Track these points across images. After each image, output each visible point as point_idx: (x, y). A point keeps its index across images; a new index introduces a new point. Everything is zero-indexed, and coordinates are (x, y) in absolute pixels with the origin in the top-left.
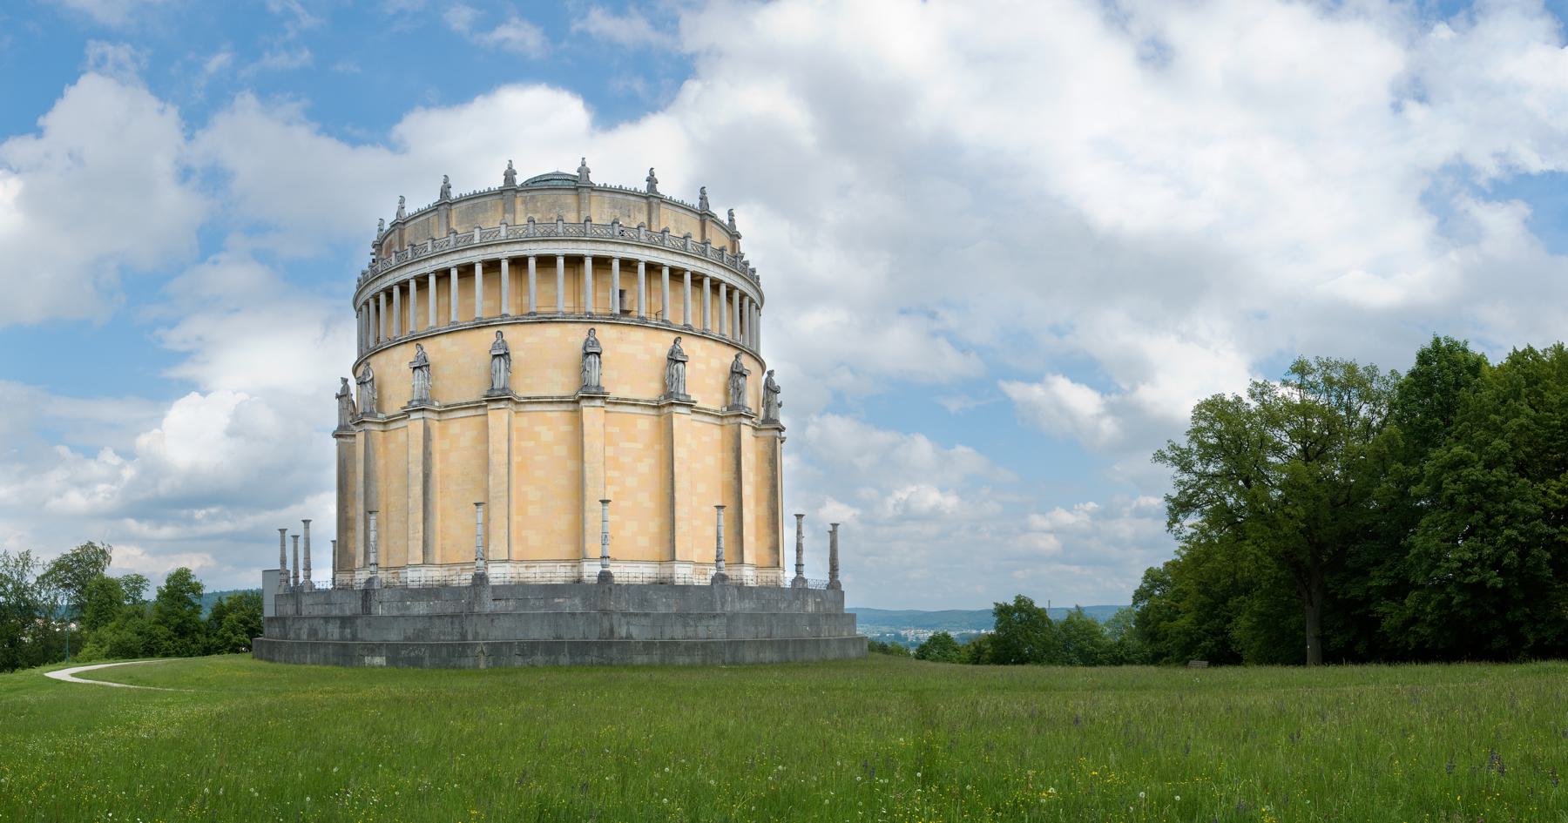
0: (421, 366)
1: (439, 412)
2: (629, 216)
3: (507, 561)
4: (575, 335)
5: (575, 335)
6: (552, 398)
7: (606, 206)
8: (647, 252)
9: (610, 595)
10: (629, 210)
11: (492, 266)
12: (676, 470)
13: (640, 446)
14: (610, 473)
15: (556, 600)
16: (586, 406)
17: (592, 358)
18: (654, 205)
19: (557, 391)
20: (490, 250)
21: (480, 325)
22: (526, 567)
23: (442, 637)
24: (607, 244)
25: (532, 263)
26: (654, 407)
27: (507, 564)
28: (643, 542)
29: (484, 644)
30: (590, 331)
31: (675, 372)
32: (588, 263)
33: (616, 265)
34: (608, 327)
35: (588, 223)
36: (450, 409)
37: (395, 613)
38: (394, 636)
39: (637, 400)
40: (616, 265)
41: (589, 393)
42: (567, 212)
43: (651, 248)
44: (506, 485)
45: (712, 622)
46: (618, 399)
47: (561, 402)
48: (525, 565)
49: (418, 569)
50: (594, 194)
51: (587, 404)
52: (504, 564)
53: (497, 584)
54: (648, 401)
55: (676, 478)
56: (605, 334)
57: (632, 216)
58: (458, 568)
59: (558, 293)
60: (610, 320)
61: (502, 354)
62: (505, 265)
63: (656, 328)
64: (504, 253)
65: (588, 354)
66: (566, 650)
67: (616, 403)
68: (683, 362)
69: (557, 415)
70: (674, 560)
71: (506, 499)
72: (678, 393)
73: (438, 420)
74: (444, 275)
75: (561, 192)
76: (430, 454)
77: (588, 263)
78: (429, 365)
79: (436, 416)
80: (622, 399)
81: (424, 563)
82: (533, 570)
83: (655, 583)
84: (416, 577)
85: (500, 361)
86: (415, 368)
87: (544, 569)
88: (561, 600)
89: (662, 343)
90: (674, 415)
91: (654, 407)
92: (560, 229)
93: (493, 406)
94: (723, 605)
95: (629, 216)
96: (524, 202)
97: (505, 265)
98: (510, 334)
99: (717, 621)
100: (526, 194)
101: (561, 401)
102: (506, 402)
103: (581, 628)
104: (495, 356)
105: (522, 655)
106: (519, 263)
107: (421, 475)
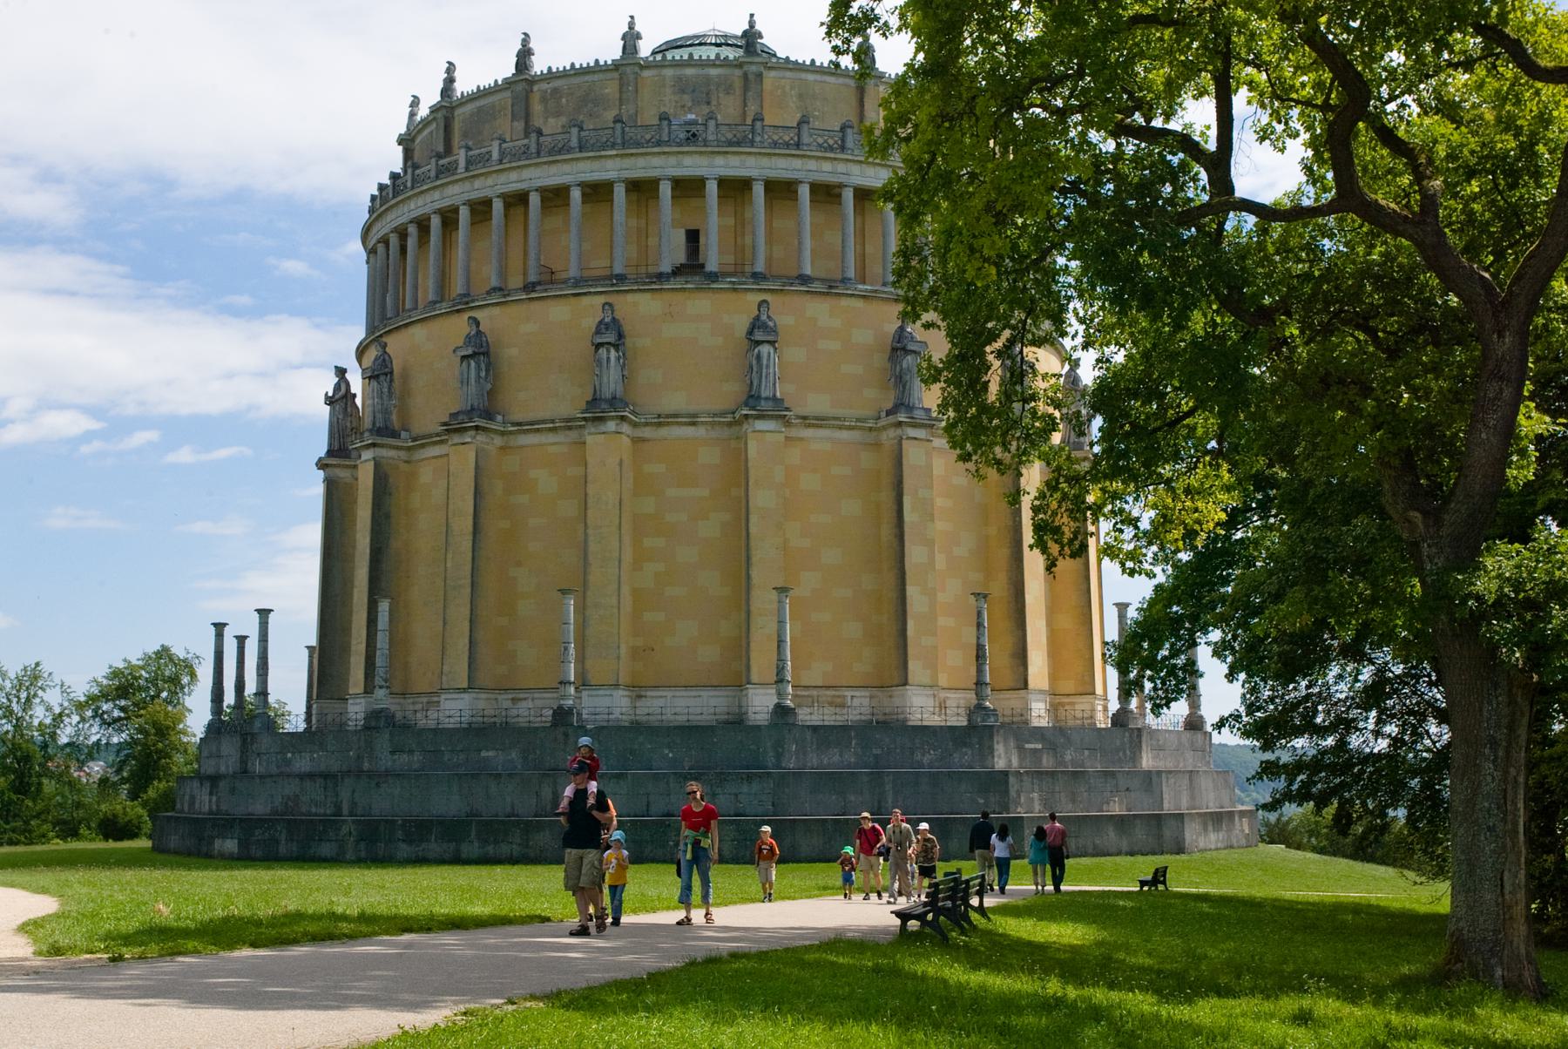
1: (409, 449)
2: (708, 103)
3: (464, 690)
4: (588, 311)
5: (588, 311)
6: (553, 421)
7: (668, 91)
8: (719, 160)
9: (566, 743)
10: (708, 94)
12: (753, 530)
13: (706, 493)
14: (648, 542)
15: (484, 754)
16: (590, 434)
17: (603, 351)
18: (751, 77)
20: (477, 183)
22: (513, 699)
23: (314, 810)
24: (648, 158)
26: (730, 424)
27: (465, 696)
28: (709, 654)
29: (353, 822)
30: (760, 306)
31: (754, 362)
32: (759, 190)
33: (804, 192)
34: (648, 296)
35: (758, 124)
36: (422, 441)
37: (274, 770)
38: (260, 808)
39: (695, 416)
40: (804, 192)
41: (600, 408)
42: (605, 109)
43: (727, 153)
44: (468, 567)
45: (745, 789)
46: (659, 416)
47: (570, 428)
48: (510, 696)
49: (358, 701)
50: (646, 73)
51: (593, 430)
52: (462, 695)
53: (451, 726)
54: (715, 415)
55: (752, 543)
56: (639, 308)
57: (714, 103)
58: (425, 700)
61: (480, 351)
63: (735, 290)
65: (598, 346)
66: (473, 833)
67: (660, 425)
68: (772, 343)
69: (555, 444)
70: (905, 683)
71: (469, 590)
72: (759, 397)
73: (406, 462)
75: (596, 77)
76: (388, 516)
77: (620, 192)
78: (392, 373)
79: (402, 454)
80: (668, 416)
81: (366, 692)
82: (523, 704)
83: (727, 722)
85: (469, 365)
86: (370, 378)
87: (539, 703)
88: (491, 753)
89: (738, 311)
90: (750, 435)
91: (730, 424)
92: (574, 142)
93: (456, 439)
94: (779, 756)
95: (708, 103)
96: (544, 100)
99: (755, 787)
100: (544, 86)
101: (569, 424)
102: (472, 433)
103: (508, 799)
104: (464, 358)
105: (409, 840)
107: (368, 551)
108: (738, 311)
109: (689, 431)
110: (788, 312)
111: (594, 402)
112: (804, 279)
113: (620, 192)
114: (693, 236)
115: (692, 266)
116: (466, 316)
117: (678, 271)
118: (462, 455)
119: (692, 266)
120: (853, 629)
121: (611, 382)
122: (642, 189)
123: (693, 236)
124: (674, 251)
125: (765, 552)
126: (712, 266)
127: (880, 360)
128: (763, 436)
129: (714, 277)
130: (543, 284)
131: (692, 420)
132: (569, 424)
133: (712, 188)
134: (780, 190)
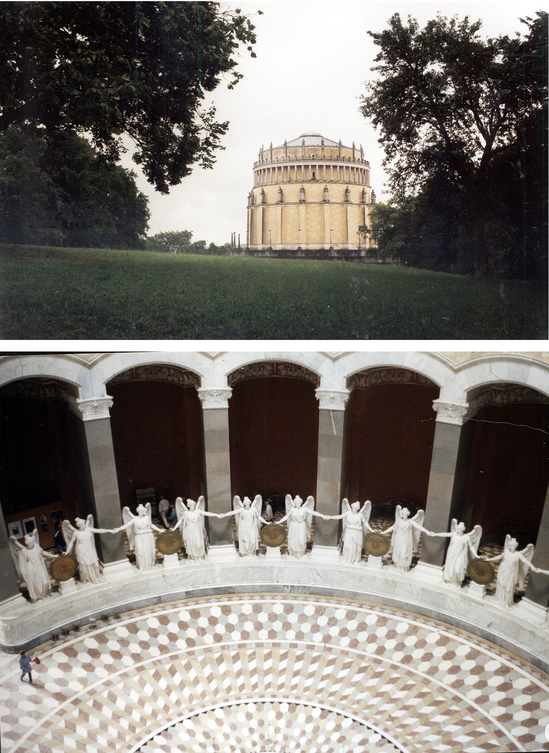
0: (263, 193)
4: (299, 186)
11: (279, 168)
13: (317, 214)
19: (295, 201)
21: (277, 183)
25: (289, 168)
56: (306, 186)
59: (294, 175)
60: (309, 182)
62: (282, 168)
64: (282, 165)
74: (269, 169)
77: (303, 167)
84: (260, 247)
89: (322, 186)
97: (282, 168)
98: (283, 187)
101: (295, 203)
106: (286, 167)
108: (322, 186)
109: (314, 205)
110: (329, 186)
111: (300, 201)
112: (332, 181)
113: (303, 167)
114: (314, 174)
115: (314, 179)
116: (278, 186)
117: (312, 179)
118: (279, 208)
119: (314, 179)
120: (339, 235)
121: (303, 198)
122: (306, 167)
123: (314, 174)
124: (310, 176)
125: (327, 224)
126: (317, 179)
127: (344, 193)
128: (326, 207)
129: (318, 181)
130: (290, 181)
131: (315, 203)
132: (295, 203)
133: (317, 167)
134: (328, 167)
